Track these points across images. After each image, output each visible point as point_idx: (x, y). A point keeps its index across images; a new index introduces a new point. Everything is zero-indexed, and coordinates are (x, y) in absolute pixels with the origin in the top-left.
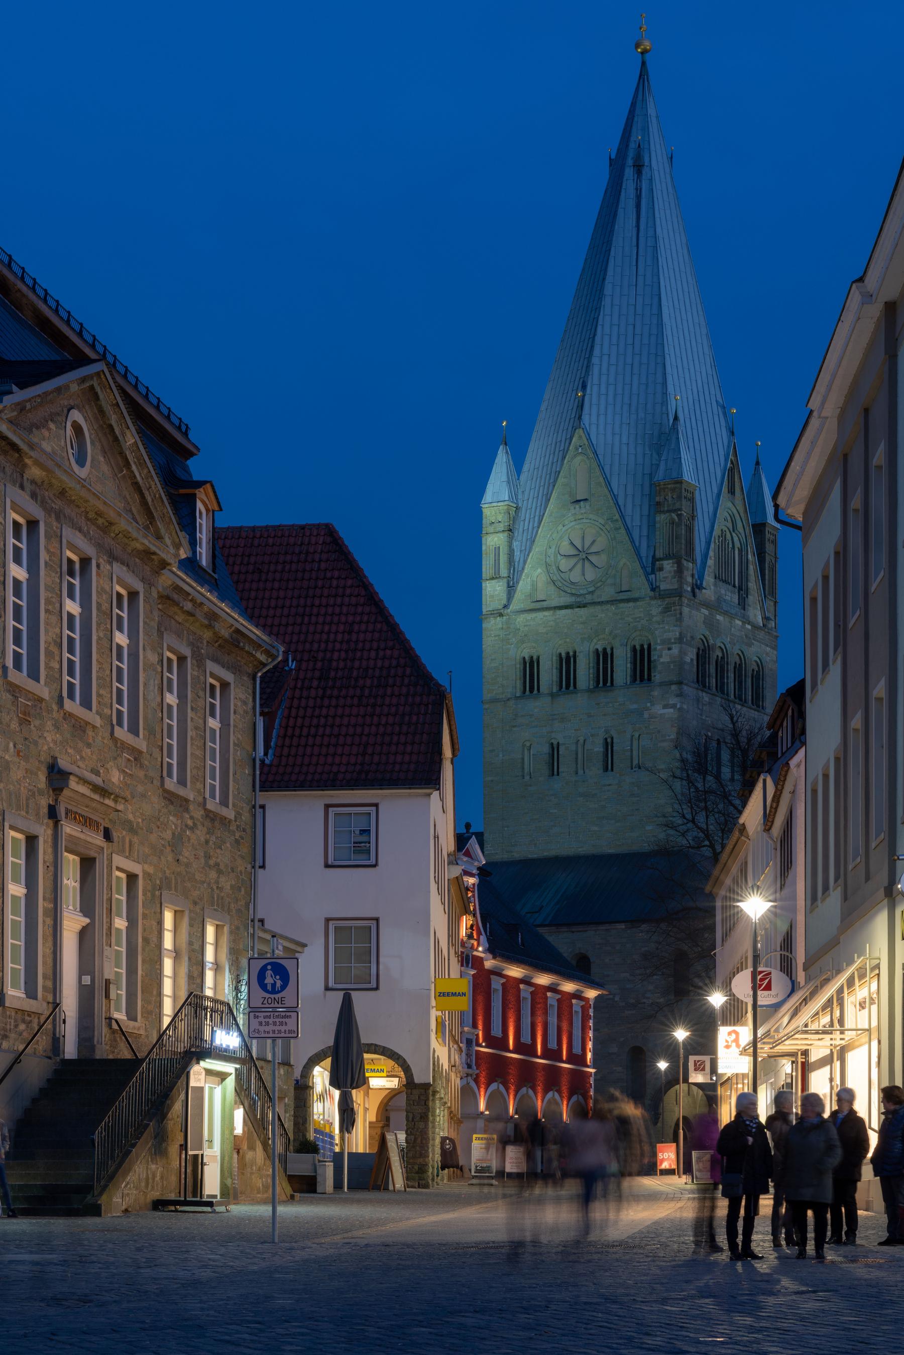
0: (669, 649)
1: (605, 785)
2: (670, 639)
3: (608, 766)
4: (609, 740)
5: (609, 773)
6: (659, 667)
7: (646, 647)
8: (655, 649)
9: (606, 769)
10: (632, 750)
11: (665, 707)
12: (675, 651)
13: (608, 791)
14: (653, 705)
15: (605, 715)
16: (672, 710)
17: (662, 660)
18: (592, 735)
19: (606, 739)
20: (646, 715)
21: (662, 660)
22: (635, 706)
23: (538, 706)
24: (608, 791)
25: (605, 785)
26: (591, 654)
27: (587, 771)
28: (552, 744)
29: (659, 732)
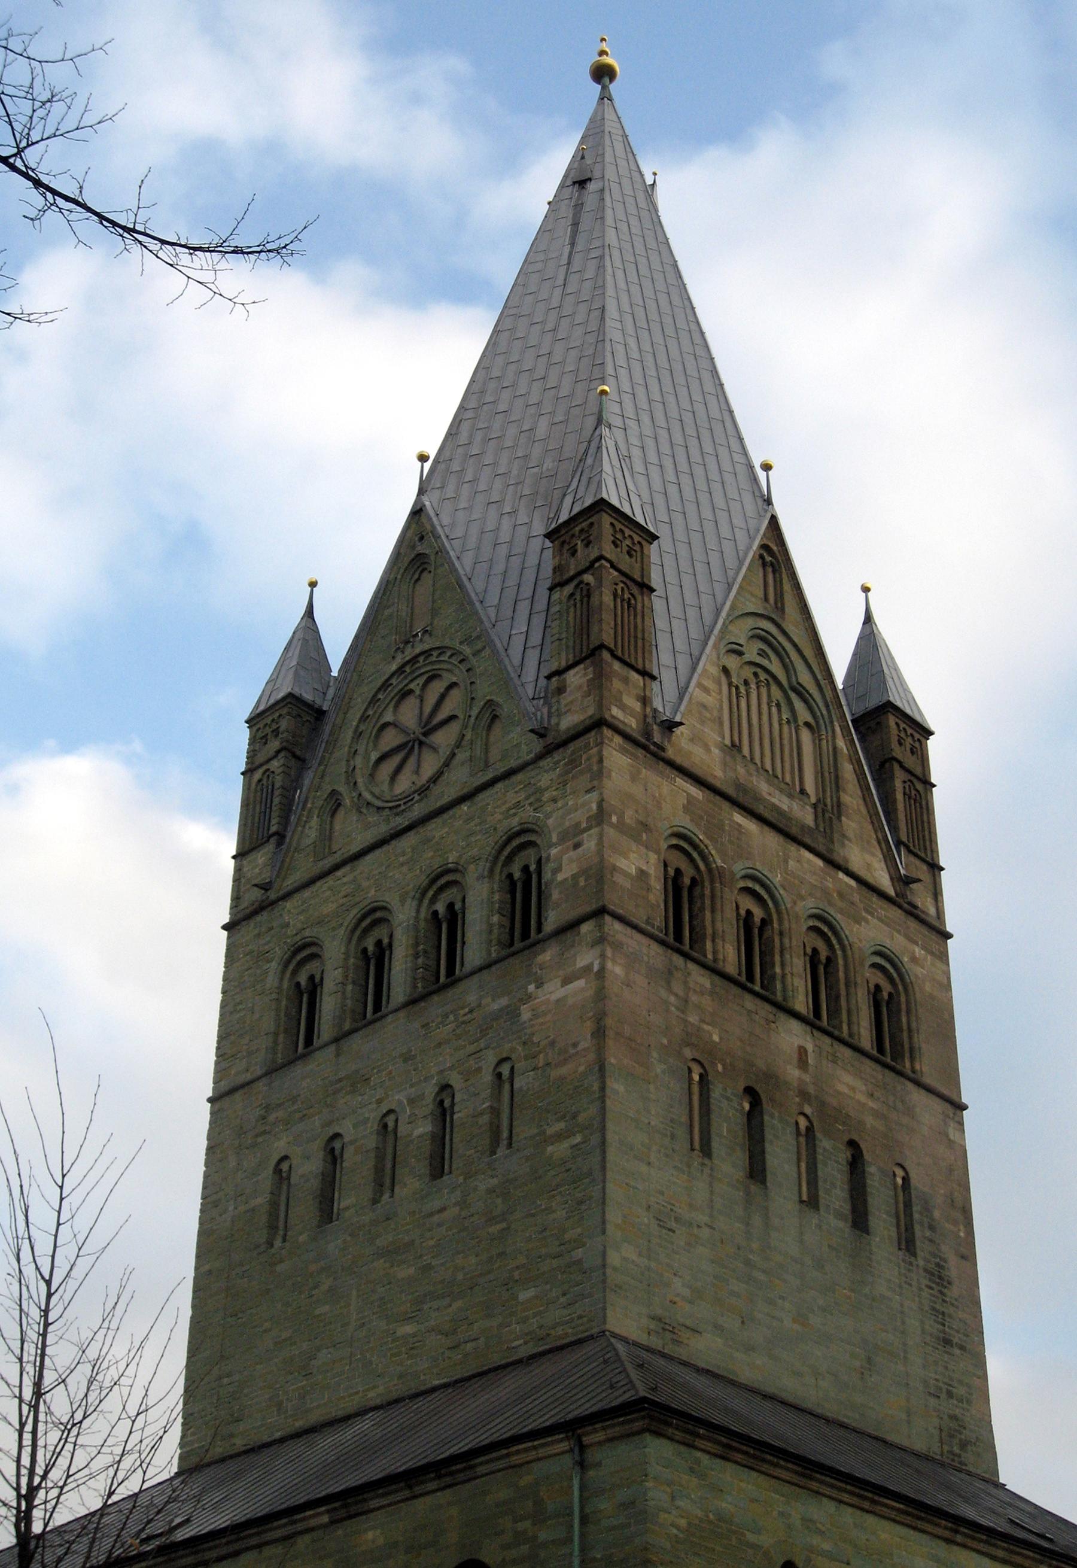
1: (432, 1214)
2: (578, 824)
4: (447, 1103)
6: (555, 895)
11: (566, 981)
12: (590, 843)
13: (439, 1225)
14: (540, 985)
15: (439, 1045)
16: (580, 983)
17: (560, 877)
20: (526, 1014)
22: (504, 1001)
24: (439, 1225)
25: (432, 1214)
26: (422, 924)
27: (397, 1189)
29: (553, 1043)
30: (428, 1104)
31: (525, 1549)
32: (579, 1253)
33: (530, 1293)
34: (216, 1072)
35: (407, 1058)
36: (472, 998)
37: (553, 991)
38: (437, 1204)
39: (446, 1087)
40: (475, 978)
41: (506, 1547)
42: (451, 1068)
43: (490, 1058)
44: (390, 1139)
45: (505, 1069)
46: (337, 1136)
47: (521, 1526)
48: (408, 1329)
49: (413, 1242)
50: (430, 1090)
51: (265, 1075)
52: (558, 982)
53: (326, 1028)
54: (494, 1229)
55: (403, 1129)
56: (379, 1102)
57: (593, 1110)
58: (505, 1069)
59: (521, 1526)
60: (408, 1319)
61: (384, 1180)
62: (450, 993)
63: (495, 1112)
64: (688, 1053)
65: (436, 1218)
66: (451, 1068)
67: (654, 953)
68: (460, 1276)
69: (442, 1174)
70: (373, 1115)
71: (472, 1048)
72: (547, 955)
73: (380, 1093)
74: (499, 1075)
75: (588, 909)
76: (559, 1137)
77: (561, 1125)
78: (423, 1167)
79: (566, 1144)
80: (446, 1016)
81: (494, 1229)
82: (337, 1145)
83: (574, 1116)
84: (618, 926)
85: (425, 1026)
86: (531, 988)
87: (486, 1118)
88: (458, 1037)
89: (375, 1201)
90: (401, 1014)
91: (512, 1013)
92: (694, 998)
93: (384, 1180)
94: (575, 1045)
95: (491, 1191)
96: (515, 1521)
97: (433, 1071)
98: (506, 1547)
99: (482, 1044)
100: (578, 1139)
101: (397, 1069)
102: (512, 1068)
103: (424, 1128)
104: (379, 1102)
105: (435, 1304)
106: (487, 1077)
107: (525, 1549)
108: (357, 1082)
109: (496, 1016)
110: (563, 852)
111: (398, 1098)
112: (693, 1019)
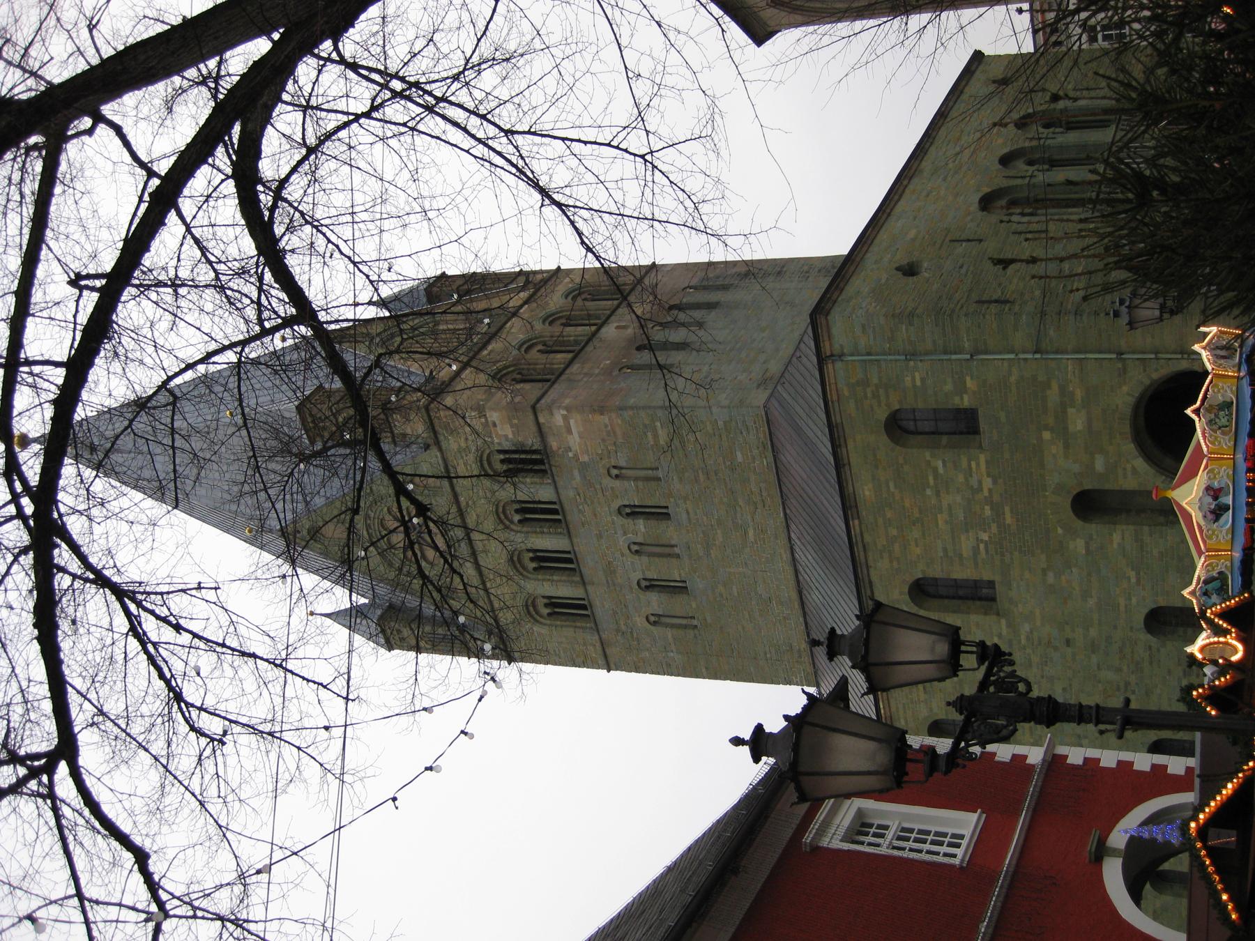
0: (495, 425)
1: (689, 519)
3: (660, 514)
4: (628, 510)
5: (670, 511)
7: (502, 457)
8: (499, 444)
9: (667, 516)
10: (636, 479)
11: (569, 431)
14: (570, 449)
16: (572, 422)
17: (511, 436)
18: (625, 533)
19: (628, 514)
20: (585, 458)
21: (511, 436)
22: (576, 473)
23: (602, 603)
27: (673, 542)
28: (647, 587)
29: (603, 440)
30: (629, 522)
31: (881, 391)
32: (720, 423)
33: (739, 455)
34: (593, 668)
35: (600, 536)
36: (571, 493)
37: (574, 440)
38: (684, 516)
39: (619, 511)
40: (560, 491)
41: (880, 405)
42: (609, 506)
43: (607, 482)
44: (646, 548)
45: (615, 472)
46: (638, 583)
47: (869, 395)
48: (751, 532)
49: (703, 532)
50: (620, 521)
51: (598, 631)
52: (569, 437)
53: (576, 592)
54: (702, 477)
55: (640, 540)
56: (623, 555)
57: (642, 414)
58: (615, 472)
59: (869, 395)
60: (746, 533)
61: (666, 551)
62: (567, 507)
63: (636, 479)
64: (616, 373)
65: (692, 515)
66: (609, 506)
67: (558, 388)
68: (725, 500)
69: (668, 514)
70: (631, 558)
71: (600, 495)
72: (554, 444)
73: (618, 555)
74: (617, 476)
75: (531, 417)
76: (656, 436)
77: (649, 434)
78: (663, 524)
79: (660, 432)
80: (580, 511)
81: (702, 477)
82: (644, 583)
83: (645, 426)
84: (543, 401)
85: (583, 524)
86: (571, 454)
87: (640, 484)
88: (592, 503)
89: (678, 556)
90: (575, 540)
91: (584, 467)
92: (585, 370)
93: (666, 551)
94: (606, 426)
95: (681, 480)
96: (866, 397)
97: (609, 519)
98: (880, 405)
99: (598, 486)
100: (658, 424)
101: (604, 543)
102: (615, 467)
103: (641, 524)
104: (623, 555)
105: (739, 515)
106: (617, 483)
107: (881, 391)
108: (610, 571)
109: (584, 477)
110: (497, 434)
111: (622, 542)
112: (597, 371)
